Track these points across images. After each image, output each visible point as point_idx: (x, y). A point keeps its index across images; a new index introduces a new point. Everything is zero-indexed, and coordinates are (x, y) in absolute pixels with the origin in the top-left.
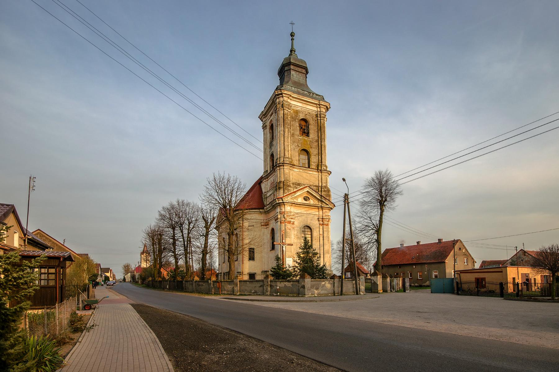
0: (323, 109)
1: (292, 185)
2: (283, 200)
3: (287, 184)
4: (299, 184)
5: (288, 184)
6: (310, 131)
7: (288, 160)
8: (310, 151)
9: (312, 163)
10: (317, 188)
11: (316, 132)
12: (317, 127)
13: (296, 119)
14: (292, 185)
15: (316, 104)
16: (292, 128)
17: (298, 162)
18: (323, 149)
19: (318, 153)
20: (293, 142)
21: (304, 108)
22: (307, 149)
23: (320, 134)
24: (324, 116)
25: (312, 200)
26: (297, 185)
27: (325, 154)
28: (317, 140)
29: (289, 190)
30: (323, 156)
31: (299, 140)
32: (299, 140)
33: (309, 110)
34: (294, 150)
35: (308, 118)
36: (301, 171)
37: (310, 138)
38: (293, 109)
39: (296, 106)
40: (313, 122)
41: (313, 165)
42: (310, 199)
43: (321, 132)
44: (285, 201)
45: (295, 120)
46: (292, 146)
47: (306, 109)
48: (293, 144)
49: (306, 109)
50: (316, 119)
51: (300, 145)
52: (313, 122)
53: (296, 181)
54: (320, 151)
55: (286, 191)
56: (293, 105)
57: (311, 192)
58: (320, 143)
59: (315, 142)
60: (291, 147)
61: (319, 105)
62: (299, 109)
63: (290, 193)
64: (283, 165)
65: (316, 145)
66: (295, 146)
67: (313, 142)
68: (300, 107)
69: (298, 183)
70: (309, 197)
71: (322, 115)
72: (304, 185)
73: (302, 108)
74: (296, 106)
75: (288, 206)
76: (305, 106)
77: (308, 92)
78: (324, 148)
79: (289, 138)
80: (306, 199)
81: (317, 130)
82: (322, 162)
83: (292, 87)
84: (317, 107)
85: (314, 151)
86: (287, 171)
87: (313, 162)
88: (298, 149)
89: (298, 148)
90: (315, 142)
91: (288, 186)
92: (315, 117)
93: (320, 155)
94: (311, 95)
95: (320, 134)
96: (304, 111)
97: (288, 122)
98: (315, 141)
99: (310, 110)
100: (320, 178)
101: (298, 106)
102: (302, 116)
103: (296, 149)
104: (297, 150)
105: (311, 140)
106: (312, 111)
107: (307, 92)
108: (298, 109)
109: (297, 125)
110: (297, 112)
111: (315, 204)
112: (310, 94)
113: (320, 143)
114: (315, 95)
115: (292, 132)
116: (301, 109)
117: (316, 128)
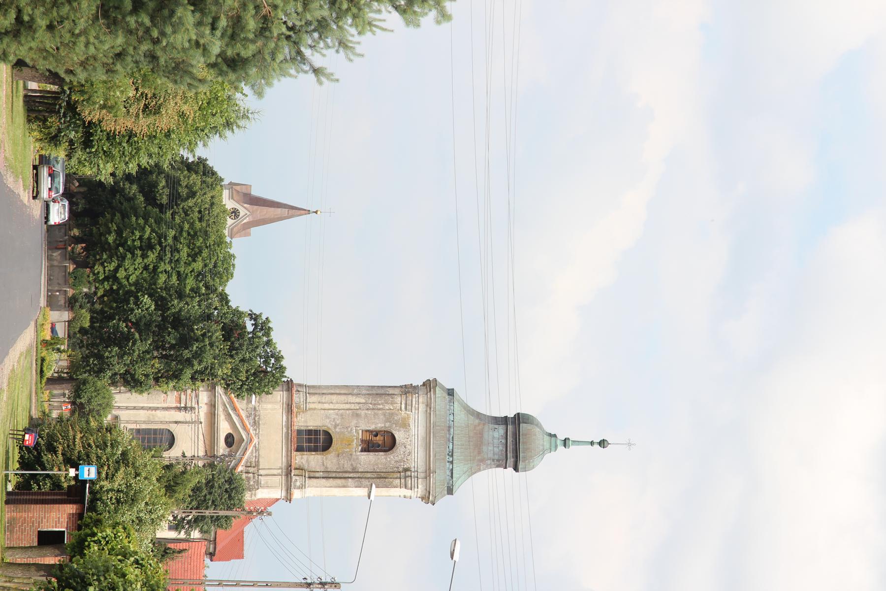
4: (256, 424)
6: (371, 453)
7: (302, 400)
9: (305, 457)
10: (254, 464)
12: (384, 471)
13: (390, 422)
16: (370, 414)
17: (303, 425)
18: (339, 482)
19: (329, 470)
20: (342, 415)
23: (369, 475)
27: (329, 485)
28: (356, 470)
30: (324, 480)
31: (349, 429)
32: (349, 429)
33: (416, 452)
35: (399, 450)
37: (358, 453)
38: (409, 418)
41: (302, 458)
45: (387, 420)
46: (332, 411)
48: (337, 414)
50: (401, 469)
51: (337, 430)
53: (262, 417)
54: (334, 475)
58: (351, 475)
59: (352, 465)
60: (329, 409)
62: (413, 431)
64: (289, 390)
66: (334, 419)
68: (416, 433)
69: (259, 423)
71: (410, 482)
72: (257, 435)
73: (416, 437)
74: (416, 424)
78: (341, 485)
79: (347, 406)
81: (378, 471)
82: (310, 478)
85: (332, 462)
88: (330, 426)
89: (332, 424)
90: (352, 465)
92: (405, 466)
93: (326, 475)
95: (369, 475)
97: (379, 404)
98: (355, 465)
99: (416, 455)
101: (416, 426)
102: (399, 436)
103: (328, 421)
105: (354, 457)
106: (416, 460)
108: (411, 427)
109: (379, 425)
113: (351, 475)
115: (363, 413)
116: (413, 433)
117: (380, 467)
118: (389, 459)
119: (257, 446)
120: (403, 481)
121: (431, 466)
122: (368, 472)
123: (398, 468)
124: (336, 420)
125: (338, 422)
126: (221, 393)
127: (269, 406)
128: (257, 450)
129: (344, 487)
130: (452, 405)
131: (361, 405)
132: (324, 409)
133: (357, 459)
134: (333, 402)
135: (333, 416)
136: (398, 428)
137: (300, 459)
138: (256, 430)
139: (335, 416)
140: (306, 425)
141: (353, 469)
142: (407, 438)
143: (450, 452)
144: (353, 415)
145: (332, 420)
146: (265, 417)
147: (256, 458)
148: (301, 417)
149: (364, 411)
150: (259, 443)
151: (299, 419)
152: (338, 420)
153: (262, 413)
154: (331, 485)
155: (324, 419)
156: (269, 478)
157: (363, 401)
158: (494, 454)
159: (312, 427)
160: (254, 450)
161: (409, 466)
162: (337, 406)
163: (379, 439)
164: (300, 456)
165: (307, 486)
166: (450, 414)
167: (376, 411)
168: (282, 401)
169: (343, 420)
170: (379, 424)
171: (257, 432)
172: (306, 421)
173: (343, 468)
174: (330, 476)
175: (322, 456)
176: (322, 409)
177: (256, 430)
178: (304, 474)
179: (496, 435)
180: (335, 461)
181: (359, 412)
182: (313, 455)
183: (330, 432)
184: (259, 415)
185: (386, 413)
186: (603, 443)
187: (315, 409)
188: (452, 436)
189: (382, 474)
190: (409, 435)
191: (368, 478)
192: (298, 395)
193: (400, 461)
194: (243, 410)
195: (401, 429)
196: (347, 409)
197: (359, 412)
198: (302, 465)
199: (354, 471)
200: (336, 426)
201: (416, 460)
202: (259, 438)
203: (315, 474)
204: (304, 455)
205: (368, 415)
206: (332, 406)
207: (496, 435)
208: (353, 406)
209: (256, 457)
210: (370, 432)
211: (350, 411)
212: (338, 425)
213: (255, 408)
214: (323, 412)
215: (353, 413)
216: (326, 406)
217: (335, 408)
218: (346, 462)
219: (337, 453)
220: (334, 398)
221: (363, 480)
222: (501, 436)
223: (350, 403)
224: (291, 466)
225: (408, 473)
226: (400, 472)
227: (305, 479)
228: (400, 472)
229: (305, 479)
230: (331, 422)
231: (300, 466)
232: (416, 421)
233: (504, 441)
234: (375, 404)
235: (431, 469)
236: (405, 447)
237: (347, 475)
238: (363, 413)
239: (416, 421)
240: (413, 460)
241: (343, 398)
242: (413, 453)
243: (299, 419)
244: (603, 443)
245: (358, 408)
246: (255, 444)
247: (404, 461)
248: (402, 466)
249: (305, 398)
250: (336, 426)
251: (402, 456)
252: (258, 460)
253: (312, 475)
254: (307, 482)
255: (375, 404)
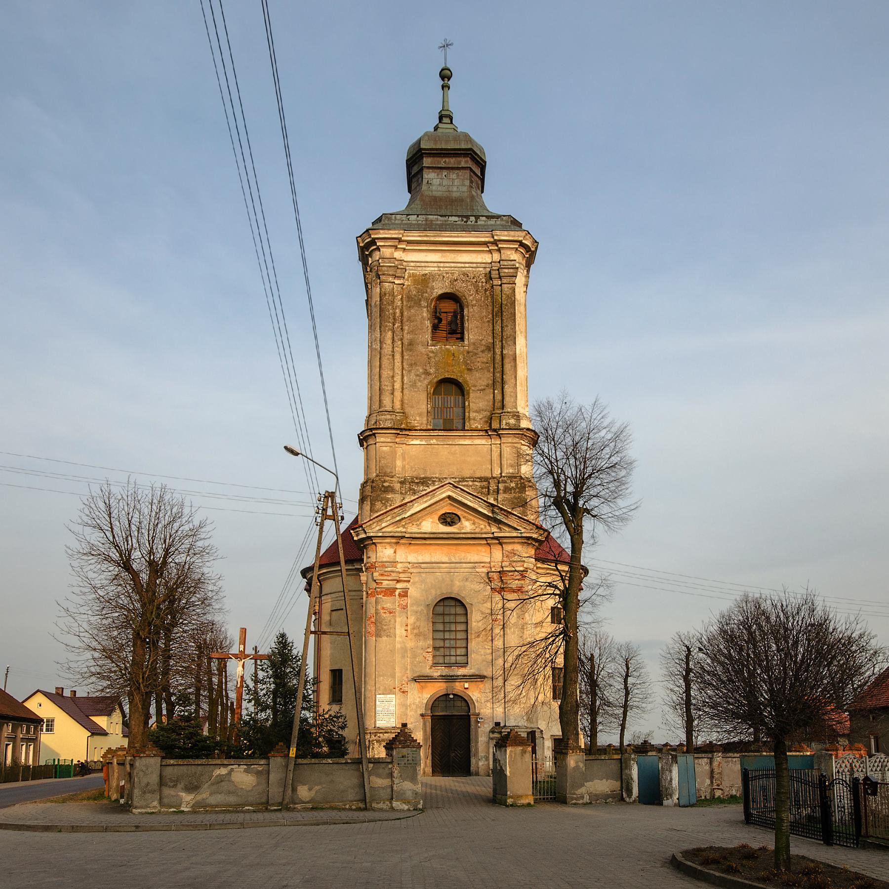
0: (509, 252)
1: (397, 486)
2: (366, 533)
3: (383, 486)
4: (424, 481)
5: (386, 484)
6: (466, 325)
7: (388, 417)
8: (466, 382)
9: (473, 415)
10: (485, 483)
11: (489, 321)
12: (490, 308)
13: (420, 300)
14: (397, 486)
15: (485, 244)
16: (409, 327)
17: (425, 419)
18: (508, 367)
19: (491, 382)
20: (411, 365)
21: (447, 265)
22: (455, 377)
23: (498, 328)
24: (511, 271)
25: (467, 520)
26: (417, 483)
27: (513, 381)
28: (491, 346)
29: (387, 500)
30: (506, 387)
31: (431, 355)
32: (431, 355)
33: (463, 265)
34: (414, 385)
35: (461, 287)
36: (434, 441)
37: (466, 342)
38: (414, 275)
39: (423, 264)
40: (478, 297)
41: (474, 419)
42: (463, 520)
43: (502, 320)
44: (372, 534)
45: (418, 303)
46: (405, 378)
47: (453, 265)
48: (410, 371)
49: (453, 265)
50: (488, 286)
51: (432, 371)
52: (478, 297)
53: (415, 474)
54: (498, 375)
55: (378, 505)
56: (412, 264)
57: (460, 498)
58: (498, 351)
59: (483, 351)
60: (403, 382)
61: (495, 243)
62: (433, 269)
63: (389, 508)
64: (374, 434)
65: (485, 360)
66: (417, 375)
67: (476, 354)
68: (435, 265)
69: (424, 478)
70: (459, 513)
71: (506, 271)
72: (440, 480)
73: (442, 265)
74: (423, 264)
75: (388, 546)
76: (450, 257)
77: (459, 216)
78: (512, 364)
79: (398, 357)
80: (448, 519)
81: (490, 316)
82: (503, 407)
83: (408, 215)
84: (490, 251)
85: (480, 378)
86: (385, 449)
87: (476, 412)
88: (426, 382)
89: (424, 379)
90: (483, 351)
91: (384, 492)
92: (484, 280)
93: (499, 386)
94: (469, 223)
95: (498, 328)
96: (447, 273)
97: (395, 313)
98: (483, 348)
99: (467, 265)
100: (496, 455)
101: (426, 264)
102: (439, 288)
103: (420, 384)
104: (424, 383)
105: (471, 349)
106: (475, 265)
107: (456, 219)
108: (427, 272)
109: (425, 315)
110: (424, 281)
111: (477, 530)
112: (466, 222)
113: (498, 351)
114: (484, 218)
115: (407, 337)
116: (436, 269)
117: (486, 313)
118: (474, 302)
119: (457, 479)
120: (504, 281)
121: (483, 240)
122: (493, 330)
123: (486, 290)
124: (418, 373)
125: (421, 371)
126: (378, 528)
127: (399, 463)
128: (463, 479)
129: (515, 359)
130: (395, 217)
131: (395, 338)
132: (403, 389)
133: (474, 344)
134: (391, 374)
135: (413, 377)
136: (429, 290)
137: (476, 420)
138: (435, 481)
139: (413, 374)
140: (426, 414)
141: (490, 350)
142: (444, 277)
143: (462, 220)
144: (411, 350)
145: (418, 378)
146: (414, 469)
147: (476, 481)
148: (414, 420)
149: (405, 335)
150: (453, 478)
151: (417, 423)
152: (418, 370)
153: (408, 474)
154: (513, 376)
155: (416, 390)
156: (504, 462)
157: (390, 334)
158: (463, 185)
159: (429, 406)
160: (464, 483)
161: (483, 275)
162: (398, 371)
163: (446, 319)
164: (472, 422)
165: (515, 410)
166: (408, 219)
167: (405, 319)
168: (391, 444)
169: (418, 364)
170: (423, 316)
171: (437, 480)
172: (420, 415)
173: (487, 363)
174: (500, 380)
175: (471, 391)
176: (402, 392)
177: (435, 481)
178: (497, 415)
179: (436, 182)
180: (478, 375)
181: (406, 342)
182: (469, 404)
183: (436, 380)
184: (412, 478)
185: (407, 305)
186: (445, 75)
187: (402, 401)
188: (439, 217)
189: (496, 309)
190: (439, 275)
191: (502, 327)
192: (381, 422)
193: (475, 285)
194: (403, 499)
195: (430, 285)
196: (403, 357)
197: (406, 342)
198: (483, 420)
199: (491, 348)
200: (427, 373)
201: (475, 265)
202: (445, 478)
203: (497, 401)
204: (469, 417)
205: (411, 329)
206: (398, 378)
207: (436, 182)
208: (398, 349)
209: (473, 481)
210: (435, 328)
211: (405, 353)
212: (426, 370)
213: (402, 483)
214: (405, 391)
215: (407, 350)
216: (398, 385)
217: (400, 373)
218: (478, 359)
219: (466, 371)
220: (386, 373)
221: (504, 334)
222: (438, 175)
223: (393, 351)
224: (486, 431)
225: (495, 274)
226: (492, 287)
227: (505, 412)
228: (492, 287)
229: (505, 412)
230: (422, 379)
231: (487, 422)
232: (418, 264)
233: (445, 173)
234: (394, 319)
235: (487, 239)
236: (456, 280)
237: (498, 357)
238: (407, 337)
239: (418, 264)
240: (474, 269)
241: (385, 362)
242: (464, 269)
243: (417, 423)
244: (445, 75)
245: (400, 342)
246: (454, 482)
247: (476, 282)
248: (484, 284)
249: (386, 413)
250: (427, 373)
251: (469, 284)
252: (478, 478)
253: (498, 405)
254: (509, 410)
255: (394, 319)
